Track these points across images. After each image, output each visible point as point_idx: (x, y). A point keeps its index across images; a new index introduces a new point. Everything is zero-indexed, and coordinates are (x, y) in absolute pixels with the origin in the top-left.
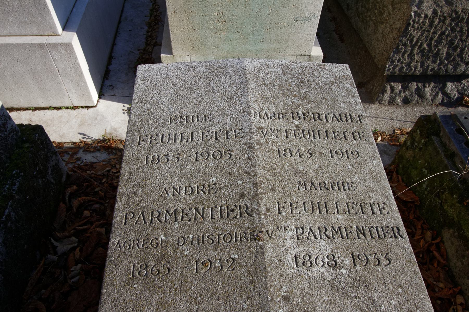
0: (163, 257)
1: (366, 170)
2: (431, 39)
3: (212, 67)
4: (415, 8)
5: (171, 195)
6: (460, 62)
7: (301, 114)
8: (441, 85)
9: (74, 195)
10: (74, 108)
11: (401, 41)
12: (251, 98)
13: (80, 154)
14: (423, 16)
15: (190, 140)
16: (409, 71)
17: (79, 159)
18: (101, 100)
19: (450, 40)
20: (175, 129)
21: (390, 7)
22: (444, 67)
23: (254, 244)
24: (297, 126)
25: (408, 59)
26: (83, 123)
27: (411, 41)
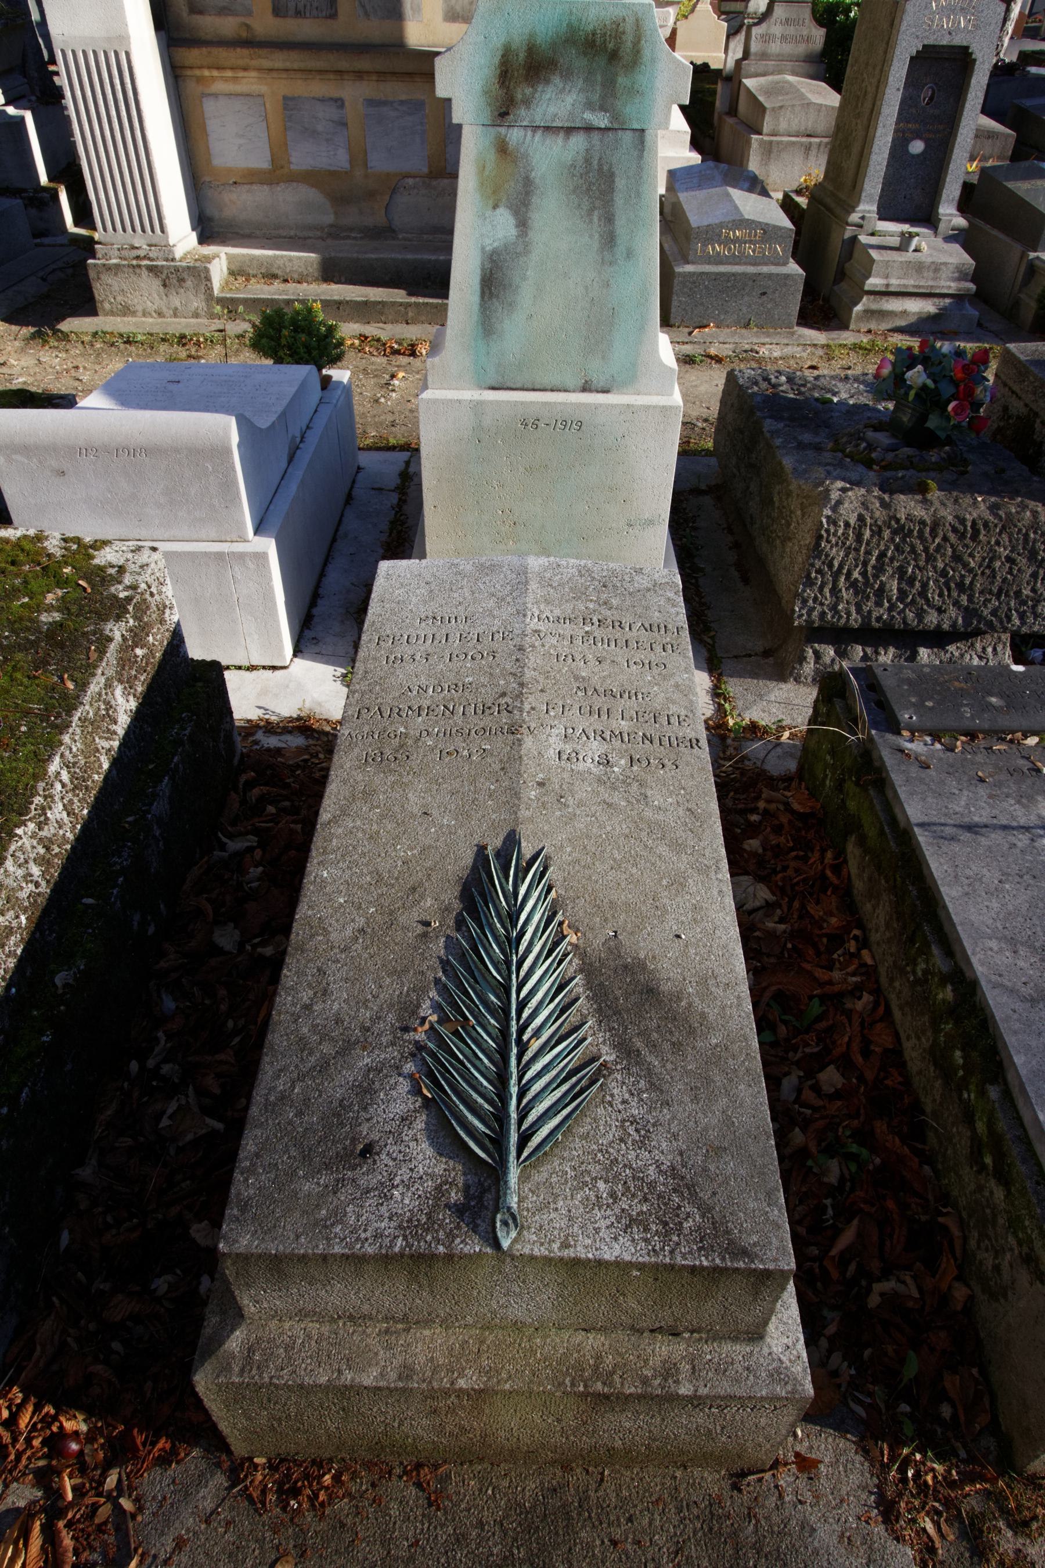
0: (401, 746)
1: (672, 682)
2: (865, 564)
3: (482, 565)
4: (827, 512)
5: (415, 692)
6: (925, 607)
7: (595, 620)
8: (908, 653)
9: (250, 785)
10: (252, 668)
11: (813, 565)
12: (530, 599)
13: (259, 735)
14: (842, 524)
15: (444, 641)
16: (838, 620)
17: (256, 742)
18: (295, 660)
19: (898, 568)
20: (426, 629)
21: (799, 513)
22: (899, 613)
23: (511, 737)
24: (587, 632)
25: (831, 597)
26: (264, 692)
27: (830, 566)
